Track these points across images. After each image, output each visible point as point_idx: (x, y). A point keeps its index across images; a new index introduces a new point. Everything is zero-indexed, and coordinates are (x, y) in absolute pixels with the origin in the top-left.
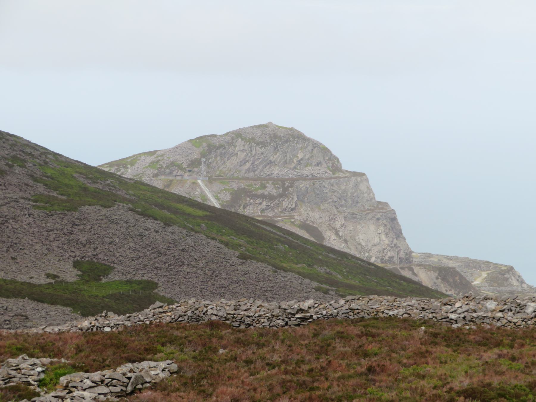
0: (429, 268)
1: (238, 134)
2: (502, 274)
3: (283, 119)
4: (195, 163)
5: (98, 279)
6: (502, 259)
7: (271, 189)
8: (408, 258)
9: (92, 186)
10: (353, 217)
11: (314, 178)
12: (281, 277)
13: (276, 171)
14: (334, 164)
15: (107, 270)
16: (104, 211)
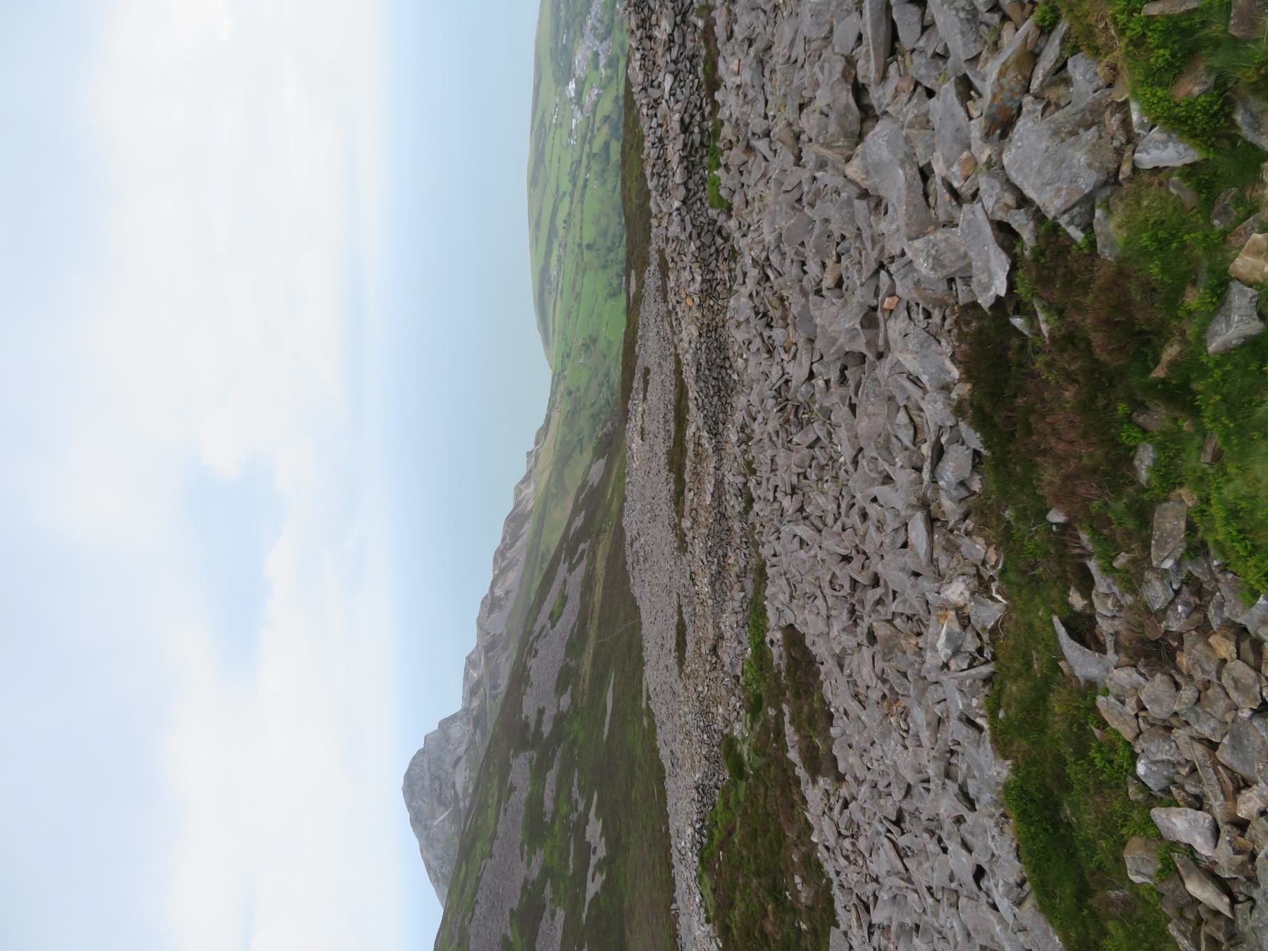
0: (470, 702)
1: (409, 806)
2: (471, 663)
3: (400, 782)
4: (425, 827)
5: (511, 944)
6: (462, 663)
7: (436, 785)
8: (466, 710)
9: (457, 940)
10: (448, 741)
11: (429, 763)
12: (500, 834)
13: (427, 783)
14: (421, 753)
15: (505, 938)
16: (472, 939)
